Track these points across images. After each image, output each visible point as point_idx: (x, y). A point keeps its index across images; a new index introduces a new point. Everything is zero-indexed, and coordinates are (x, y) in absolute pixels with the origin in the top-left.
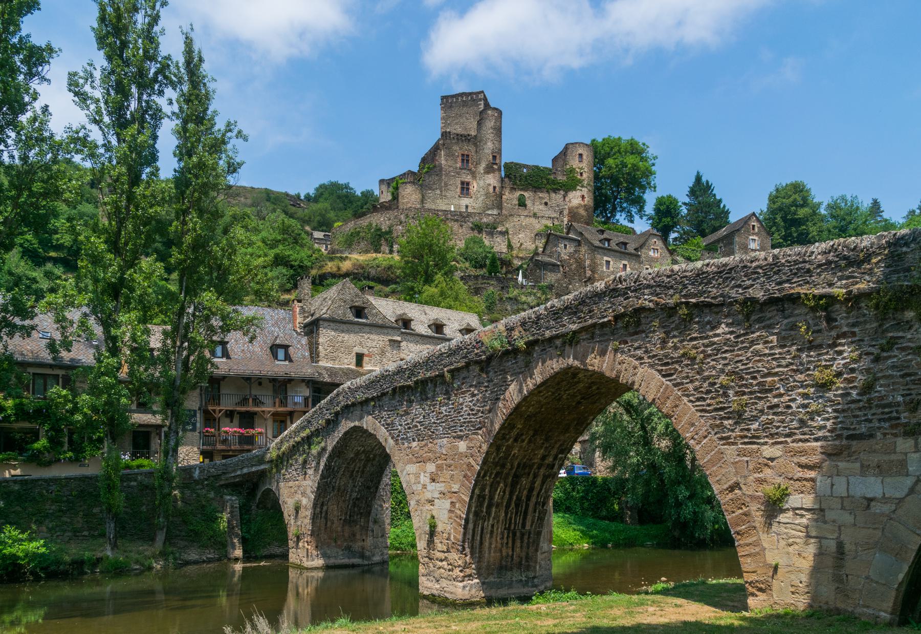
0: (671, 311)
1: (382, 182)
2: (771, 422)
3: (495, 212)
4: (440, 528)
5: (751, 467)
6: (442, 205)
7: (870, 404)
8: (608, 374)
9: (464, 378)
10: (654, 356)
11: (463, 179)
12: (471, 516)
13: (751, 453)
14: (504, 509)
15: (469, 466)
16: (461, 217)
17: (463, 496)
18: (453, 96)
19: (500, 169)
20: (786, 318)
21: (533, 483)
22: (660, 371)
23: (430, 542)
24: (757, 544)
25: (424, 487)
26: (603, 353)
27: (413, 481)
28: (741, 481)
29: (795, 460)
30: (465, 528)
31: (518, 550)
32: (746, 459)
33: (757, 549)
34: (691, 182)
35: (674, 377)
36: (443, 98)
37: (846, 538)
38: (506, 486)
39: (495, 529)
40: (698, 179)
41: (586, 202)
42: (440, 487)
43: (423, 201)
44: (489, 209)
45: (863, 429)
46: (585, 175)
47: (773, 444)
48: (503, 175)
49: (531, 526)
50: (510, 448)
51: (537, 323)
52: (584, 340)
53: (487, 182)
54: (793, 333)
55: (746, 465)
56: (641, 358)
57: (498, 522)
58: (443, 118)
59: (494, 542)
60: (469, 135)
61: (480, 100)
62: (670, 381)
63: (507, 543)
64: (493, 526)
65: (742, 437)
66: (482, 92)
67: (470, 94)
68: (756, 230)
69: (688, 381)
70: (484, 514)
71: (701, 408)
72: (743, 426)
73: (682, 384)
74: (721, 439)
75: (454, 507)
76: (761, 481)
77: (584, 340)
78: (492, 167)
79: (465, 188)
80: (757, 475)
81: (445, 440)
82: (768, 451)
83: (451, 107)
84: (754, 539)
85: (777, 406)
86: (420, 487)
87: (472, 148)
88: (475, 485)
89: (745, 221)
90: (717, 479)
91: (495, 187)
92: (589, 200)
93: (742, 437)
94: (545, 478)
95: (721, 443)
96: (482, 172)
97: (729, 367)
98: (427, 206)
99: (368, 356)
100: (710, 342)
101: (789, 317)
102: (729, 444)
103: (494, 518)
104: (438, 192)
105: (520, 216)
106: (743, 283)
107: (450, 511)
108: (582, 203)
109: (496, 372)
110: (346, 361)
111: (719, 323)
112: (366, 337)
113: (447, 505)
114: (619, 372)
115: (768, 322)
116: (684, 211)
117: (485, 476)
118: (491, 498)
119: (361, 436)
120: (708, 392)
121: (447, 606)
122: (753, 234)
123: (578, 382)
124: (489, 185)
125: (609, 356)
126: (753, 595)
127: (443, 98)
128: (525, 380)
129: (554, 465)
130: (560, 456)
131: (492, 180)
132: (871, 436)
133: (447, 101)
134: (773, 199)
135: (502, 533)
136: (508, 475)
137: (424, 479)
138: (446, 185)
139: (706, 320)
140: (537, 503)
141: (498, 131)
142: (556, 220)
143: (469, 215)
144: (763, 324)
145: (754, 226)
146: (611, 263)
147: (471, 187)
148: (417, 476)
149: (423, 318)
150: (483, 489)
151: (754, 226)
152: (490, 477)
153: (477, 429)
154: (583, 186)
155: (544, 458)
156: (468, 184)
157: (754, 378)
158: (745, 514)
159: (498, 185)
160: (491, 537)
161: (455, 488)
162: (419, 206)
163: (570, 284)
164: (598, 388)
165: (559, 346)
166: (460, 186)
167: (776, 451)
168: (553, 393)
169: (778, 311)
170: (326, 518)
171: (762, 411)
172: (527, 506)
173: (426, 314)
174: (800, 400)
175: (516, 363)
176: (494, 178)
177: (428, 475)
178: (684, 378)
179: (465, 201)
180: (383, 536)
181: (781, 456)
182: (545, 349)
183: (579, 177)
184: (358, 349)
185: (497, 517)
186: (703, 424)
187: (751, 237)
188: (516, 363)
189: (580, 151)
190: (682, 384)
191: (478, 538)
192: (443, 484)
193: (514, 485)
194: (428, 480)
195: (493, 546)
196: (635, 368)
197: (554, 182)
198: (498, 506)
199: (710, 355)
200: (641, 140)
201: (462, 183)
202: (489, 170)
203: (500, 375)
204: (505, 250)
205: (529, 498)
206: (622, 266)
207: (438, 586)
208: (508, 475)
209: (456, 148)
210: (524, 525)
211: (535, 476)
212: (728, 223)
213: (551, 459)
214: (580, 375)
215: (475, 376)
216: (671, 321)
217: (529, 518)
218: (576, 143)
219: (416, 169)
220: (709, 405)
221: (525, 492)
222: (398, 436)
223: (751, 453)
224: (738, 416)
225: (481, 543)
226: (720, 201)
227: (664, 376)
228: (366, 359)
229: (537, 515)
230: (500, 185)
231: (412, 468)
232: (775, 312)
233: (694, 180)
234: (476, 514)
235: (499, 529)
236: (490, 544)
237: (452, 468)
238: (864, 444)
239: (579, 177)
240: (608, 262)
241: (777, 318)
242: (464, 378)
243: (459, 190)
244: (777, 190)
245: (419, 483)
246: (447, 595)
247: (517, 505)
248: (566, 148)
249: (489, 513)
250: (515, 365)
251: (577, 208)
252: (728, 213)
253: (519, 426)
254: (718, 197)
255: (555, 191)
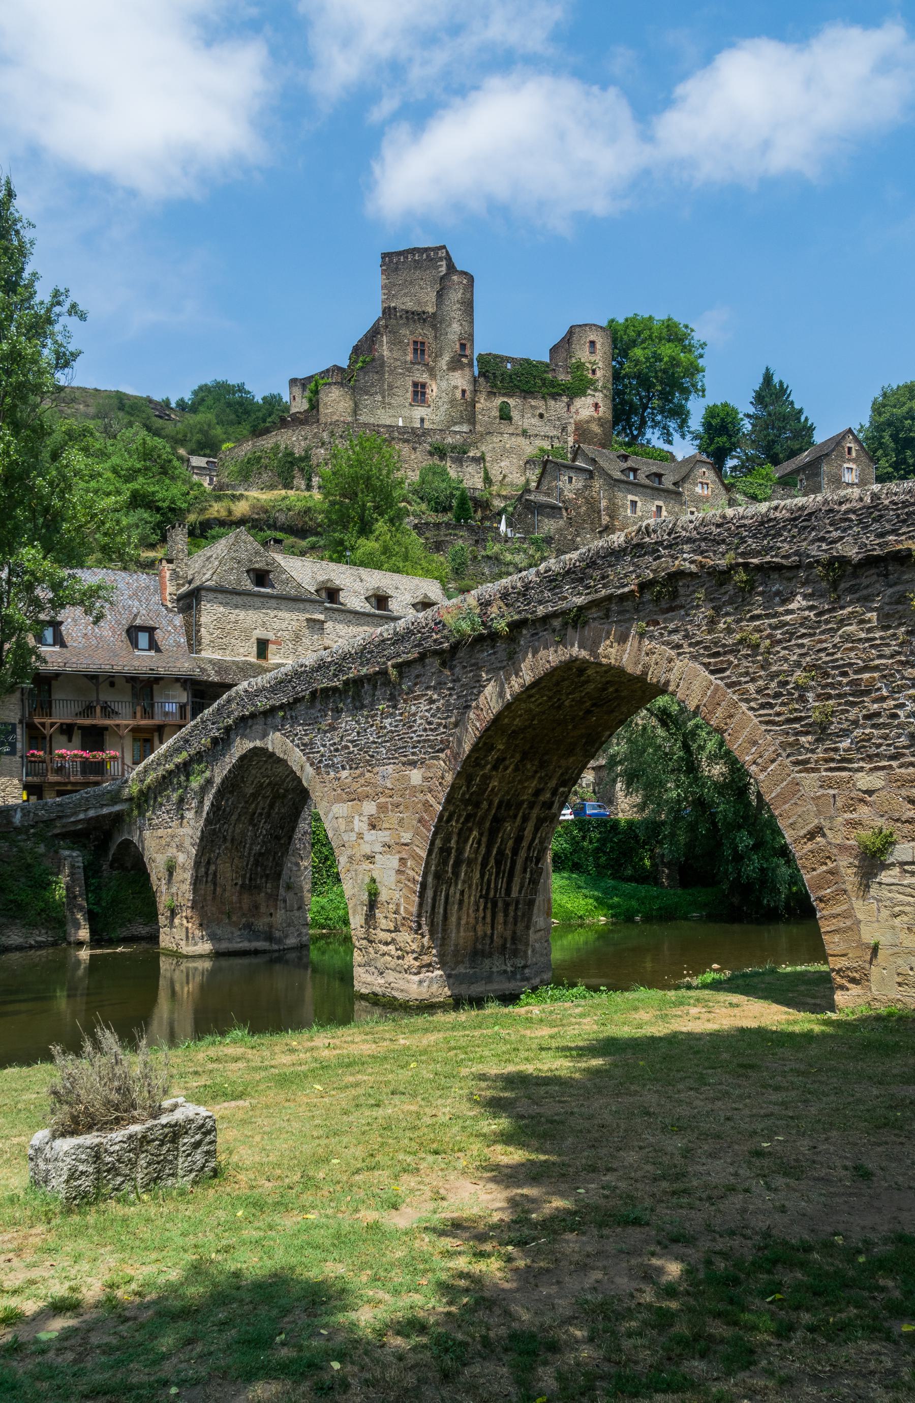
0: (722, 576)
1: (293, 382)
2: (869, 739)
3: (465, 428)
4: (383, 897)
5: (839, 804)
6: (384, 418)
8: (630, 669)
9: (417, 676)
10: (698, 643)
11: (416, 379)
12: (430, 879)
13: (839, 784)
14: (479, 868)
15: (427, 805)
16: (414, 436)
17: (418, 850)
18: (399, 254)
19: (471, 365)
20: (891, 586)
21: (522, 829)
22: (707, 666)
23: (370, 917)
24: (848, 914)
25: (360, 836)
26: (622, 639)
27: (343, 828)
28: (826, 824)
29: (904, 792)
30: (422, 895)
31: (500, 928)
32: (832, 792)
33: (849, 923)
34: (757, 383)
35: (728, 673)
36: (385, 256)
38: (481, 834)
39: (466, 896)
40: (768, 378)
41: (601, 414)
42: (384, 836)
43: (355, 412)
44: (455, 424)
46: (599, 374)
47: (871, 770)
48: (476, 373)
49: (520, 892)
50: (486, 778)
51: (524, 595)
52: (594, 619)
53: (453, 383)
54: (900, 607)
55: (832, 800)
56: (678, 646)
57: (470, 887)
58: (384, 287)
59: (464, 917)
60: (424, 313)
61: (441, 259)
62: (722, 679)
63: (484, 918)
64: (462, 892)
65: (827, 761)
66: (444, 247)
67: (426, 250)
68: (854, 454)
69: (747, 679)
70: (450, 875)
71: (767, 718)
72: (828, 744)
73: (739, 683)
74: (796, 763)
75: (405, 865)
76: (854, 824)
77: (594, 619)
78: (460, 361)
79: (419, 393)
80: (848, 816)
82: (864, 781)
83: (396, 269)
84: (845, 907)
85: (877, 714)
86: (353, 836)
87: (429, 333)
88: (435, 834)
89: (838, 441)
90: (791, 821)
91: (464, 392)
92: (605, 411)
93: (827, 761)
94: (540, 822)
95: (796, 769)
96: (445, 368)
97: (808, 659)
98: (362, 419)
99: (274, 643)
100: (780, 622)
101: (895, 584)
102: (807, 770)
103: (464, 882)
104: (379, 398)
105: (502, 434)
106: (827, 536)
107: (399, 872)
108: (595, 415)
109: (465, 667)
110: (242, 650)
111: (793, 594)
112: (272, 615)
113: (394, 862)
114: (646, 667)
115: (865, 592)
116: (747, 426)
117: (449, 820)
118: (460, 851)
119: (266, 762)
120: (777, 695)
121: (395, 1009)
122: (849, 460)
123: (587, 682)
124: (456, 387)
125: (631, 644)
126: (842, 988)
127: (385, 256)
128: (508, 679)
129: (552, 803)
130: (562, 789)
131: (460, 380)
133: (391, 261)
134: (877, 409)
135: (477, 904)
136: (483, 819)
137: (360, 825)
138: (391, 387)
139: (774, 589)
140: (528, 859)
141: (468, 306)
142: (556, 440)
143: (426, 433)
144: (857, 596)
145: (850, 449)
146: (639, 504)
147: (428, 391)
148: (349, 820)
149: (358, 586)
150: (447, 839)
151: (850, 449)
152: (457, 822)
153: (438, 751)
154: (596, 390)
155: (538, 793)
156: (424, 386)
157: (844, 674)
158: (831, 872)
159: (468, 388)
160: (460, 908)
161: (406, 837)
162: (350, 419)
163: (578, 535)
164: (617, 691)
165: (558, 628)
166: (411, 389)
167: (876, 780)
168: (550, 698)
169: (878, 575)
170: (215, 884)
171: (855, 723)
172: (513, 863)
173: (362, 581)
175: (494, 653)
176: (463, 377)
177: (365, 819)
178: (741, 675)
179: (420, 412)
180: (300, 908)
181: (883, 788)
182: (537, 634)
183: (590, 376)
184: (259, 633)
185: (469, 878)
186: (770, 742)
187: (846, 465)
188: (494, 653)
189: (592, 338)
190: (739, 683)
191: (441, 911)
192: (387, 833)
193: (493, 833)
194: (365, 826)
195: (463, 922)
196: (670, 660)
197: (553, 384)
198: (470, 862)
199: (779, 642)
200: (680, 319)
201: (415, 385)
202: (456, 364)
203: (471, 671)
204: (480, 485)
205: (515, 852)
206: (654, 509)
207: (382, 981)
208: (483, 819)
209: (404, 331)
210: (508, 891)
211: (525, 819)
212: (811, 444)
213: (548, 795)
214: (590, 672)
215: (433, 674)
216: (723, 591)
217: (517, 880)
218: (586, 325)
219: (345, 364)
220: (778, 714)
221: (510, 843)
222: (320, 761)
223: (839, 784)
224: (821, 731)
225: (445, 918)
226: (800, 411)
227: (712, 672)
228: (272, 648)
229: (528, 876)
230: (471, 388)
231: (340, 809)
232: (875, 578)
233: (761, 380)
234: (438, 876)
235: (472, 898)
236: (459, 919)
237: (402, 808)
239: (590, 376)
240: (634, 503)
241: (877, 586)
242: (417, 676)
243: (409, 395)
244: (885, 395)
245: (352, 830)
246: (396, 994)
247: (498, 863)
248: (571, 332)
249: (456, 874)
250: (493, 657)
251: (588, 422)
252: (811, 429)
253: (501, 747)
254: (797, 406)
255: (555, 396)
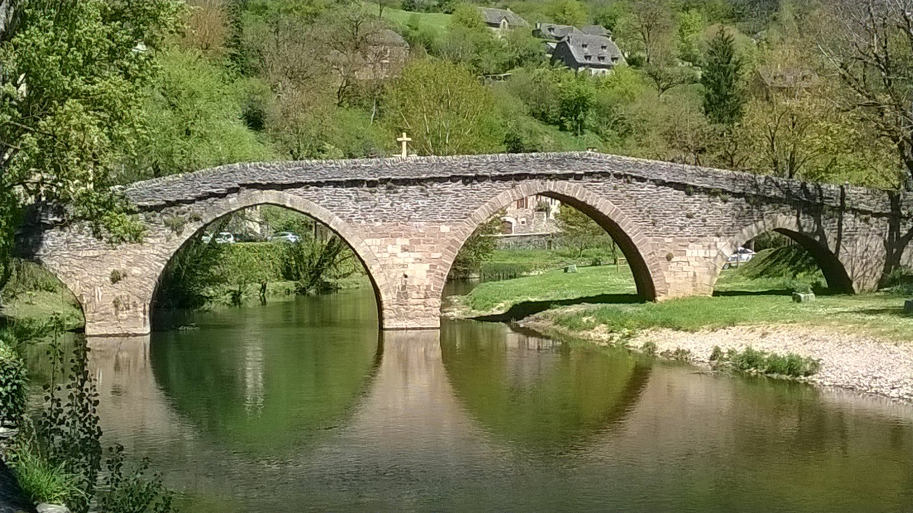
7: (705, 226)
8: (579, 199)
13: (659, 240)
17: (445, 261)
22: (613, 202)
28: (655, 251)
37: (696, 271)
45: (703, 234)
72: (655, 229)
81: (422, 224)
82: (666, 240)
107: (428, 271)
113: (427, 266)
132: (706, 236)
167: (670, 240)
171: (664, 224)
174: (680, 221)
194: (397, 250)
196: (598, 198)
223: (659, 240)
237: (432, 242)
238: (704, 238)
